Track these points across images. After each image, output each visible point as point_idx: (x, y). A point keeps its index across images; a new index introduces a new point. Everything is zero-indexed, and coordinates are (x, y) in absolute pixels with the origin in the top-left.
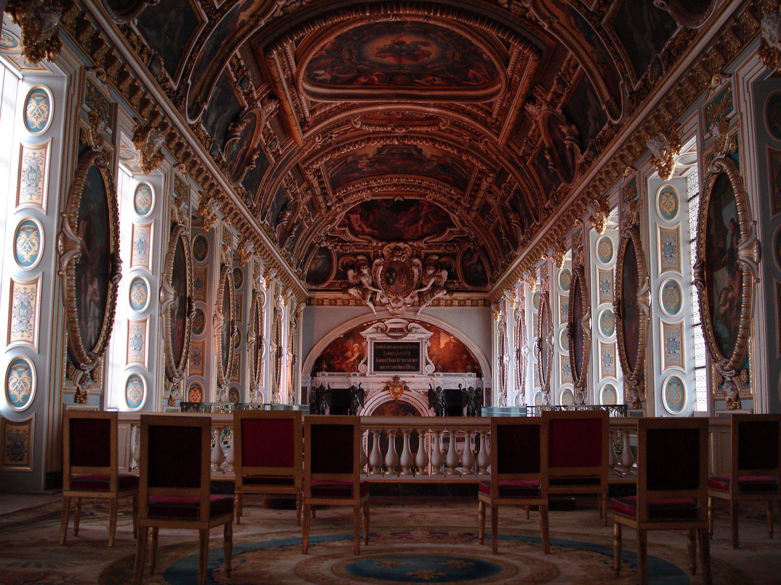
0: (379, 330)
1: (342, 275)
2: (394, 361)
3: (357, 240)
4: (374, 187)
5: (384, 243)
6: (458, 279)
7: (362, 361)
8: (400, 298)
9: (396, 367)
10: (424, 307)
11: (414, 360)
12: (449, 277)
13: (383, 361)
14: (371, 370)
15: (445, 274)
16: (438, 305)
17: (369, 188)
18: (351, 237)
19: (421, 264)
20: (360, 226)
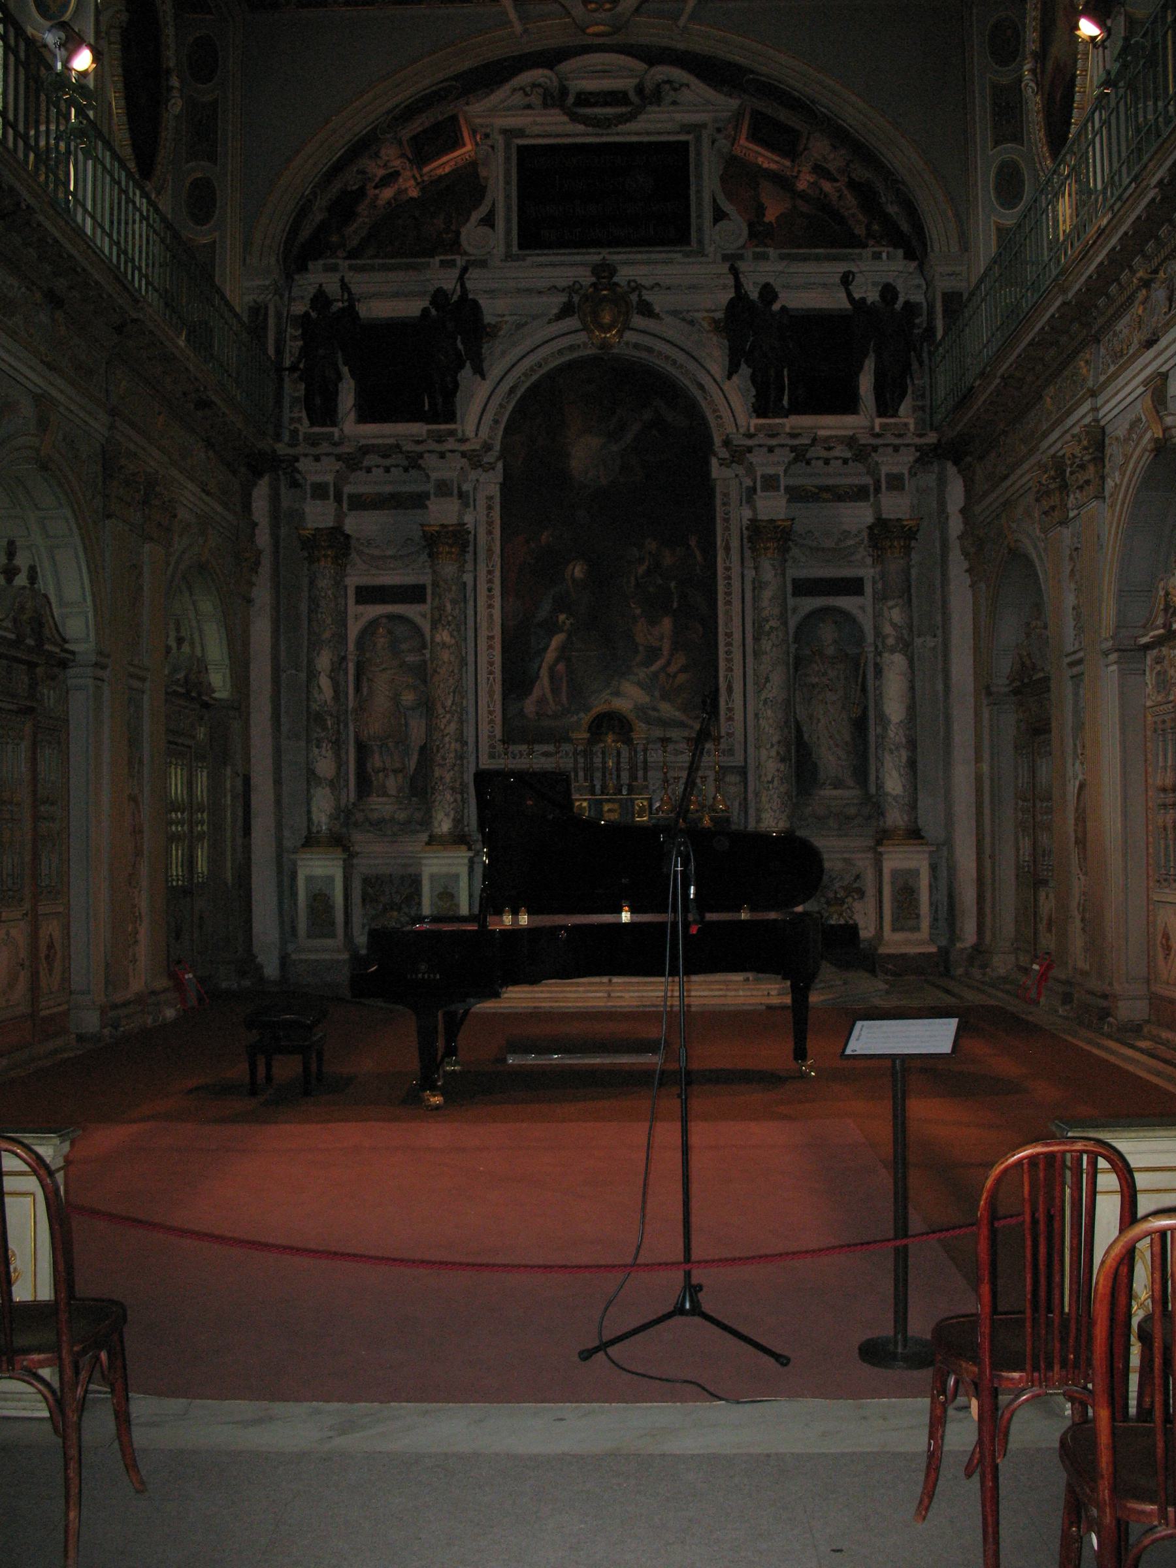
0: (536, 100)
7: (476, 216)
14: (508, 245)
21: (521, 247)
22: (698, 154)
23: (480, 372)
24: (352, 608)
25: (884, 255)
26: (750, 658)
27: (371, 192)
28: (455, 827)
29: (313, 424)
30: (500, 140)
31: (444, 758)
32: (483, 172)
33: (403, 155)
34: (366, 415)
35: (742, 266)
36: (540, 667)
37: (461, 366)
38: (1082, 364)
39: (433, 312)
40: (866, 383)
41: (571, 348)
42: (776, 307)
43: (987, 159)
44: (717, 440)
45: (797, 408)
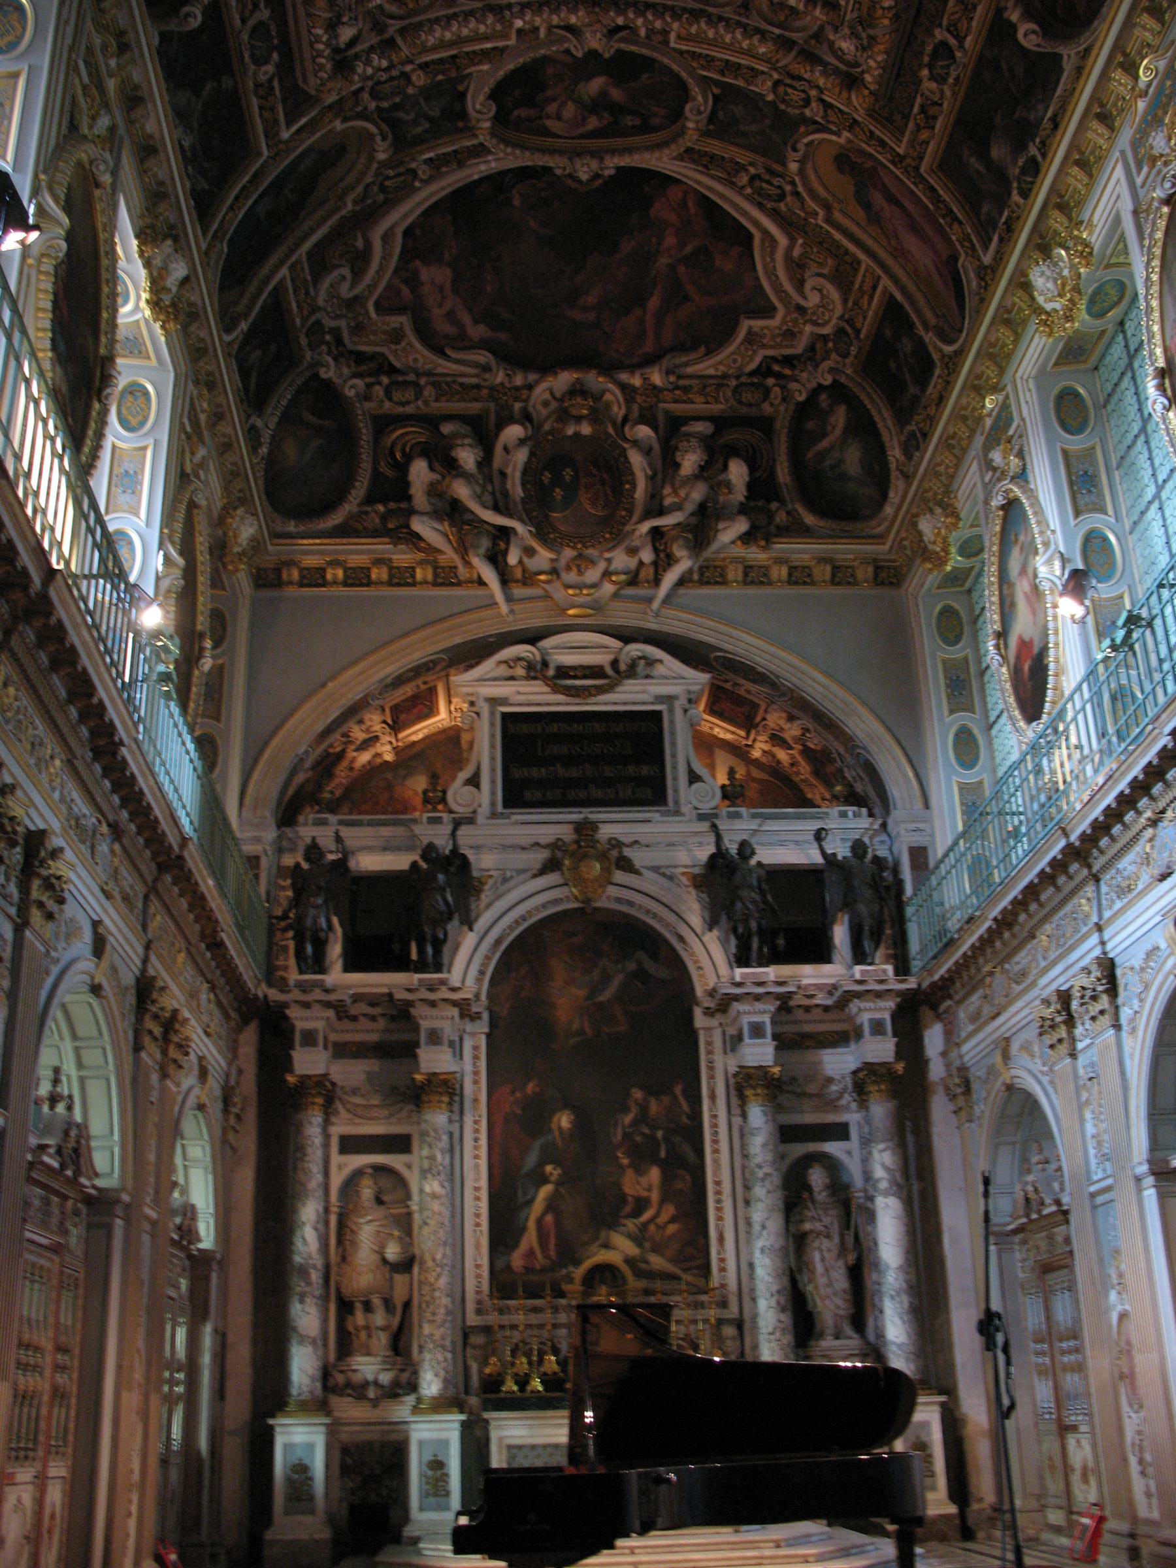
0: (520, 671)
1: (392, 490)
2: (574, 772)
3: (444, 366)
5: (532, 377)
6: (782, 502)
7: (463, 775)
8: (591, 552)
9: (582, 795)
10: (670, 578)
11: (645, 770)
12: (750, 486)
13: (535, 772)
14: (493, 804)
15: (737, 472)
16: (721, 581)
18: (419, 355)
19: (657, 447)
20: (451, 316)
21: (506, 805)
22: (672, 722)
23: (469, 924)
24: (336, 1158)
25: (850, 814)
26: (740, 1204)
27: (351, 754)
28: (445, 1388)
29: (301, 972)
30: (485, 709)
31: (434, 1314)
32: (465, 738)
33: (384, 722)
34: (353, 964)
35: (722, 825)
36: (527, 1219)
37: (450, 918)
38: (1083, 901)
39: (424, 865)
40: (840, 934)
41: (556, 901)
42: (753, 862)
43: (940, 728)
44: (699, 992)
45: (777, 957)
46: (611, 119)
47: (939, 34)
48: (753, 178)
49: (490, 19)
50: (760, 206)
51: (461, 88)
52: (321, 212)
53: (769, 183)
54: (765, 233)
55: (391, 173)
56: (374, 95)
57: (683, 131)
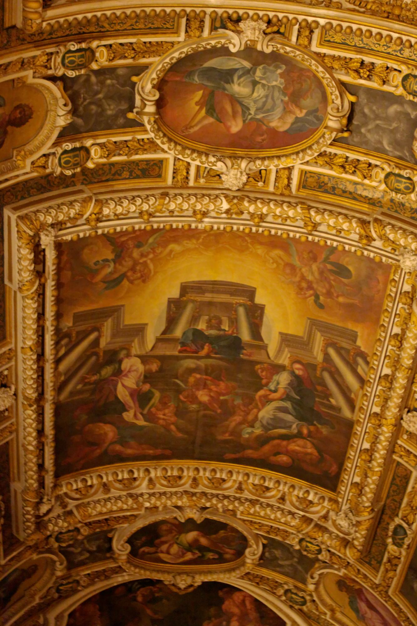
4: (142, 495)
17: (131, 496)
46: (200, 554)
47: (398, 521)
48: (287, 592)
49: (130, 501)
50: (291, 607)
51: (110, 535)
52: (19, 604)
53: (296, 594)
54: (294, 622)
55: (64, 582)
56: (57, 539)
57: (244, 564)
